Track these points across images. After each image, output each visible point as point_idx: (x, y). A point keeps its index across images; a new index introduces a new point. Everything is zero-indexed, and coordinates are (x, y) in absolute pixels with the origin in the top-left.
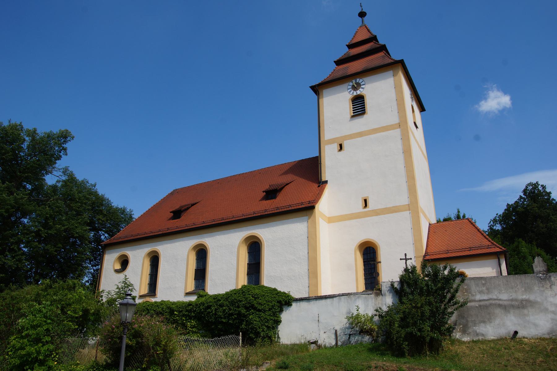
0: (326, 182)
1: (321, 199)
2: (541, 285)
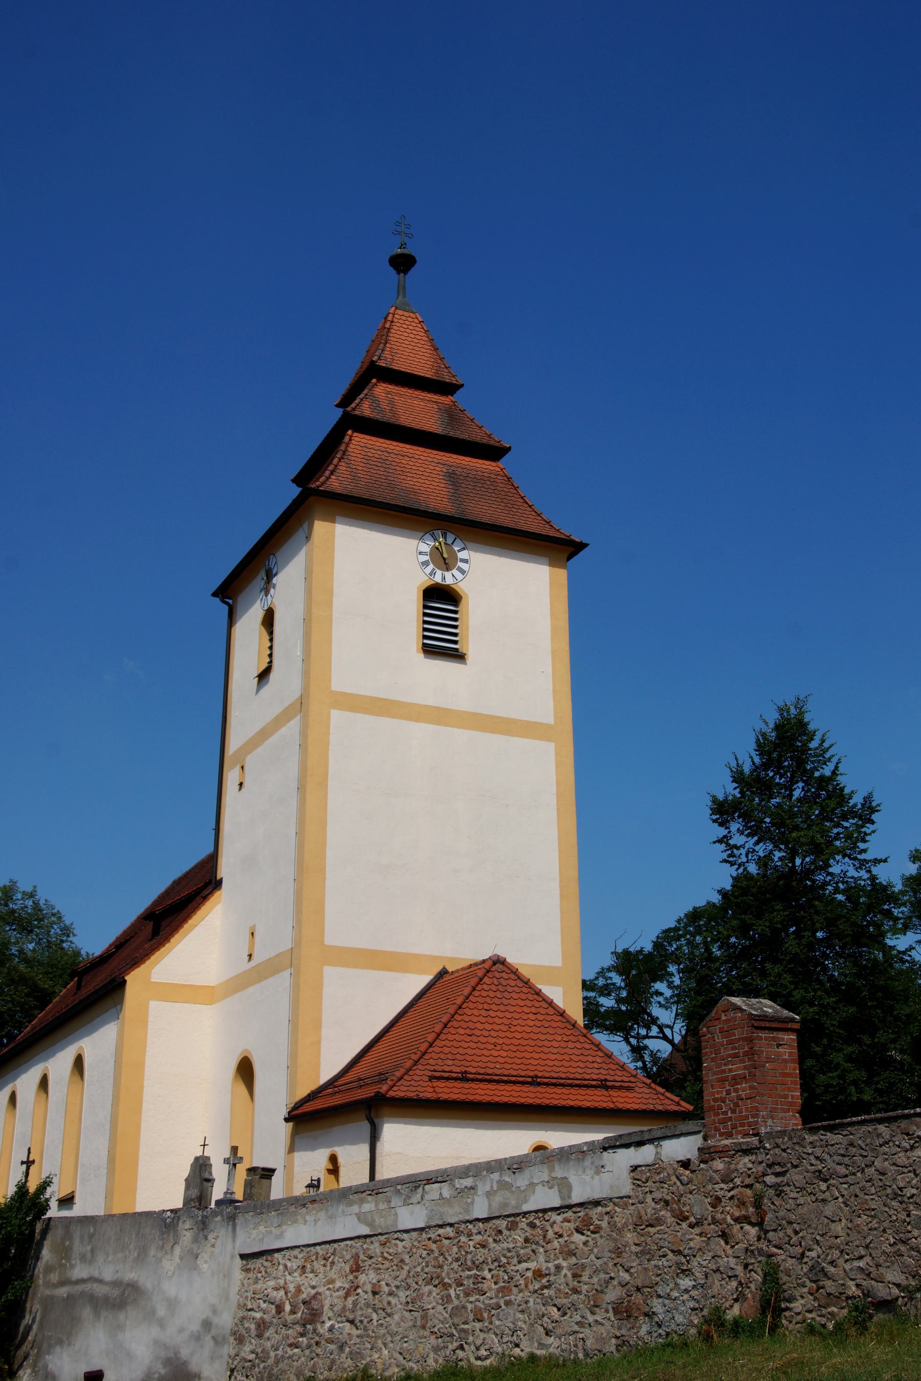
0: (218, 884)
1: (167, 945)
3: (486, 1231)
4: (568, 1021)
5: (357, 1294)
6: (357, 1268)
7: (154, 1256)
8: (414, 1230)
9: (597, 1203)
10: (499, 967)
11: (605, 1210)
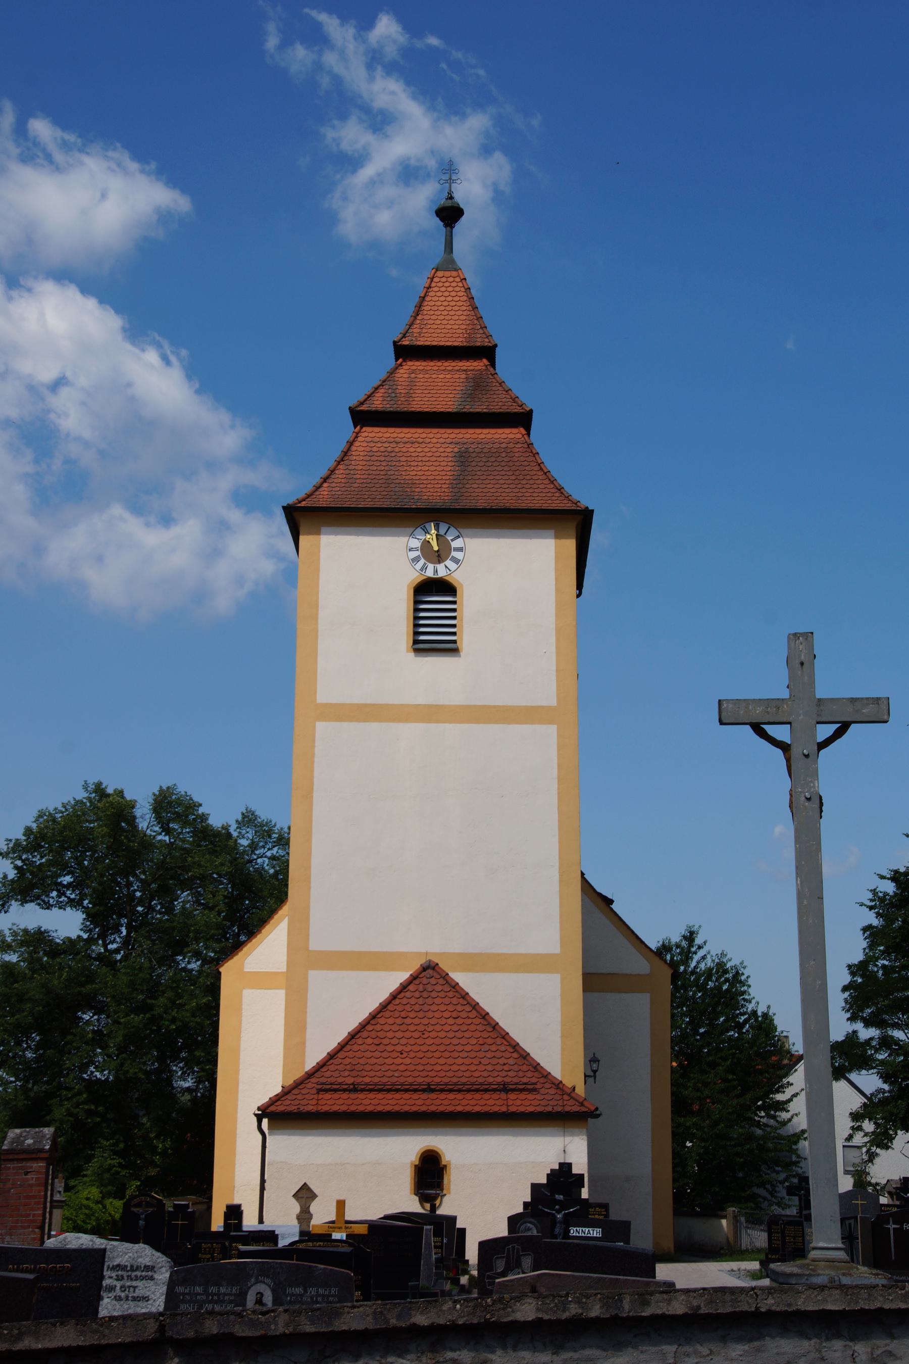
4: (489, 1024)
10: (430, 972)
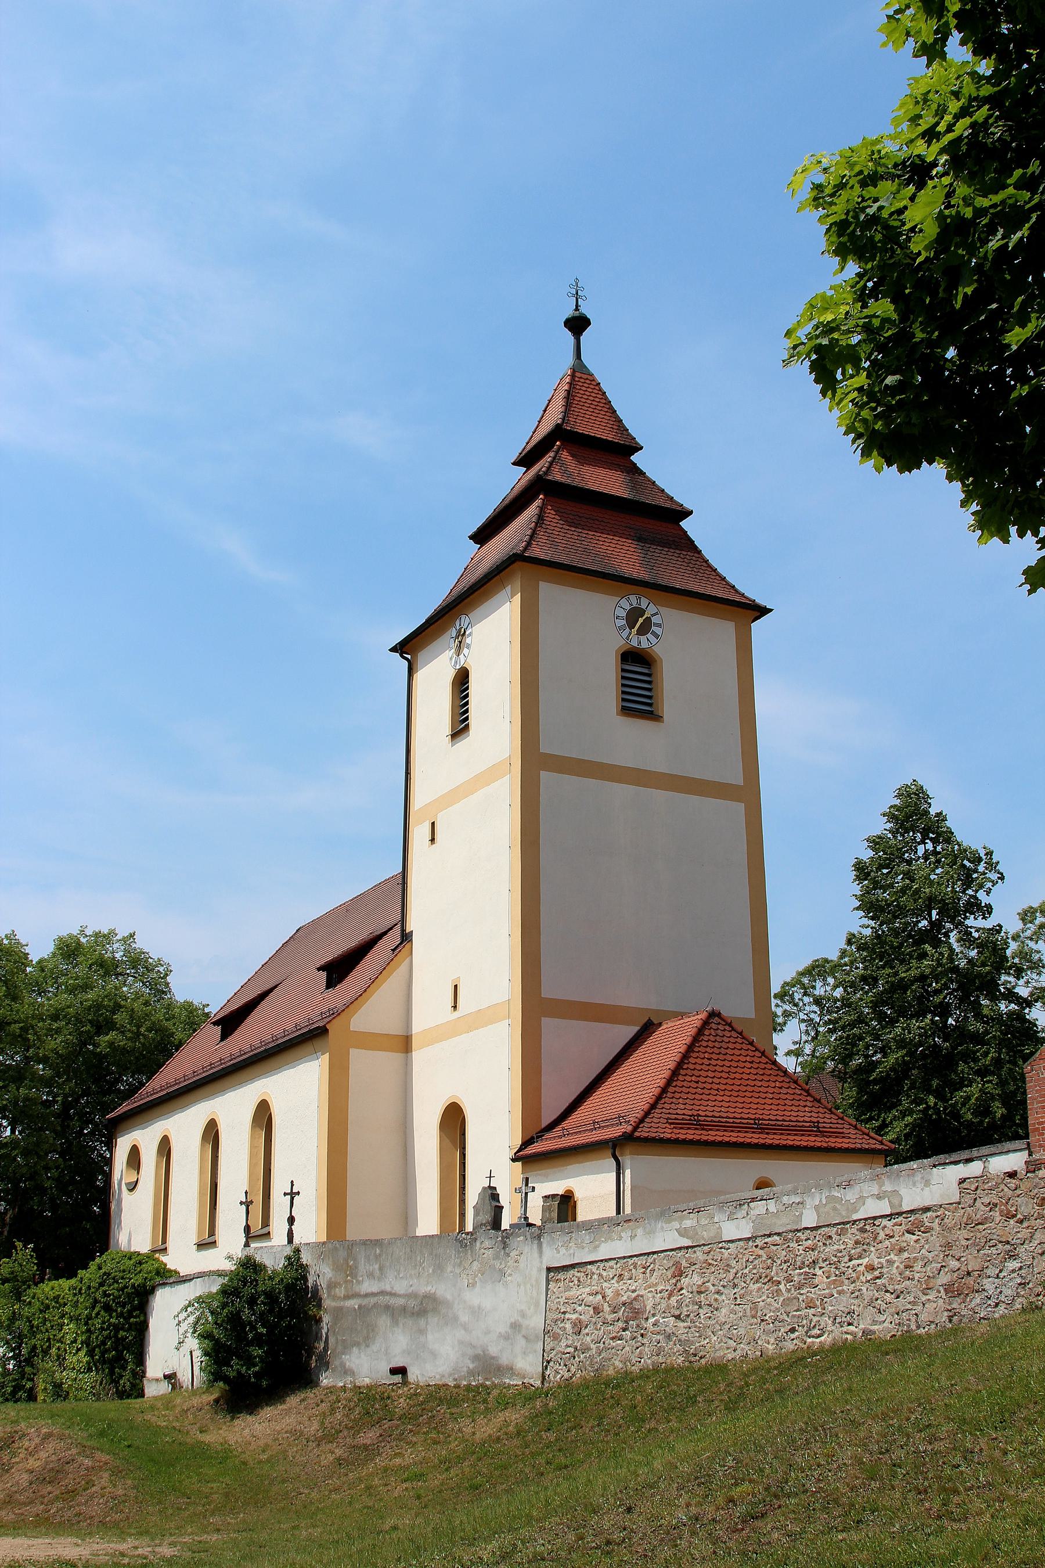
2: (459, 1261)
3: (815, 1237)
5: (681, 1295)
6: (679, 1273)
7: (451, 1272)
8: (740, 1240)
9: (926, 1209)
10: (716, 1019)
11: (934, 1214)
